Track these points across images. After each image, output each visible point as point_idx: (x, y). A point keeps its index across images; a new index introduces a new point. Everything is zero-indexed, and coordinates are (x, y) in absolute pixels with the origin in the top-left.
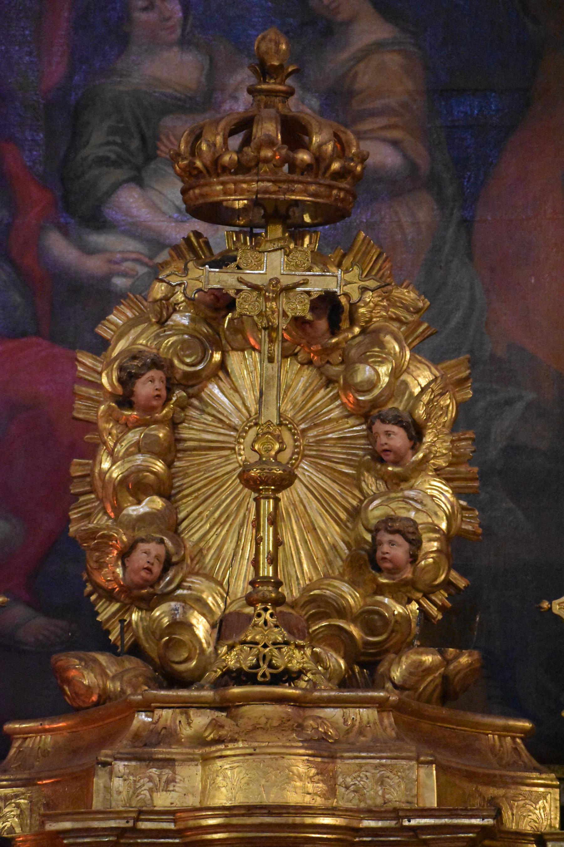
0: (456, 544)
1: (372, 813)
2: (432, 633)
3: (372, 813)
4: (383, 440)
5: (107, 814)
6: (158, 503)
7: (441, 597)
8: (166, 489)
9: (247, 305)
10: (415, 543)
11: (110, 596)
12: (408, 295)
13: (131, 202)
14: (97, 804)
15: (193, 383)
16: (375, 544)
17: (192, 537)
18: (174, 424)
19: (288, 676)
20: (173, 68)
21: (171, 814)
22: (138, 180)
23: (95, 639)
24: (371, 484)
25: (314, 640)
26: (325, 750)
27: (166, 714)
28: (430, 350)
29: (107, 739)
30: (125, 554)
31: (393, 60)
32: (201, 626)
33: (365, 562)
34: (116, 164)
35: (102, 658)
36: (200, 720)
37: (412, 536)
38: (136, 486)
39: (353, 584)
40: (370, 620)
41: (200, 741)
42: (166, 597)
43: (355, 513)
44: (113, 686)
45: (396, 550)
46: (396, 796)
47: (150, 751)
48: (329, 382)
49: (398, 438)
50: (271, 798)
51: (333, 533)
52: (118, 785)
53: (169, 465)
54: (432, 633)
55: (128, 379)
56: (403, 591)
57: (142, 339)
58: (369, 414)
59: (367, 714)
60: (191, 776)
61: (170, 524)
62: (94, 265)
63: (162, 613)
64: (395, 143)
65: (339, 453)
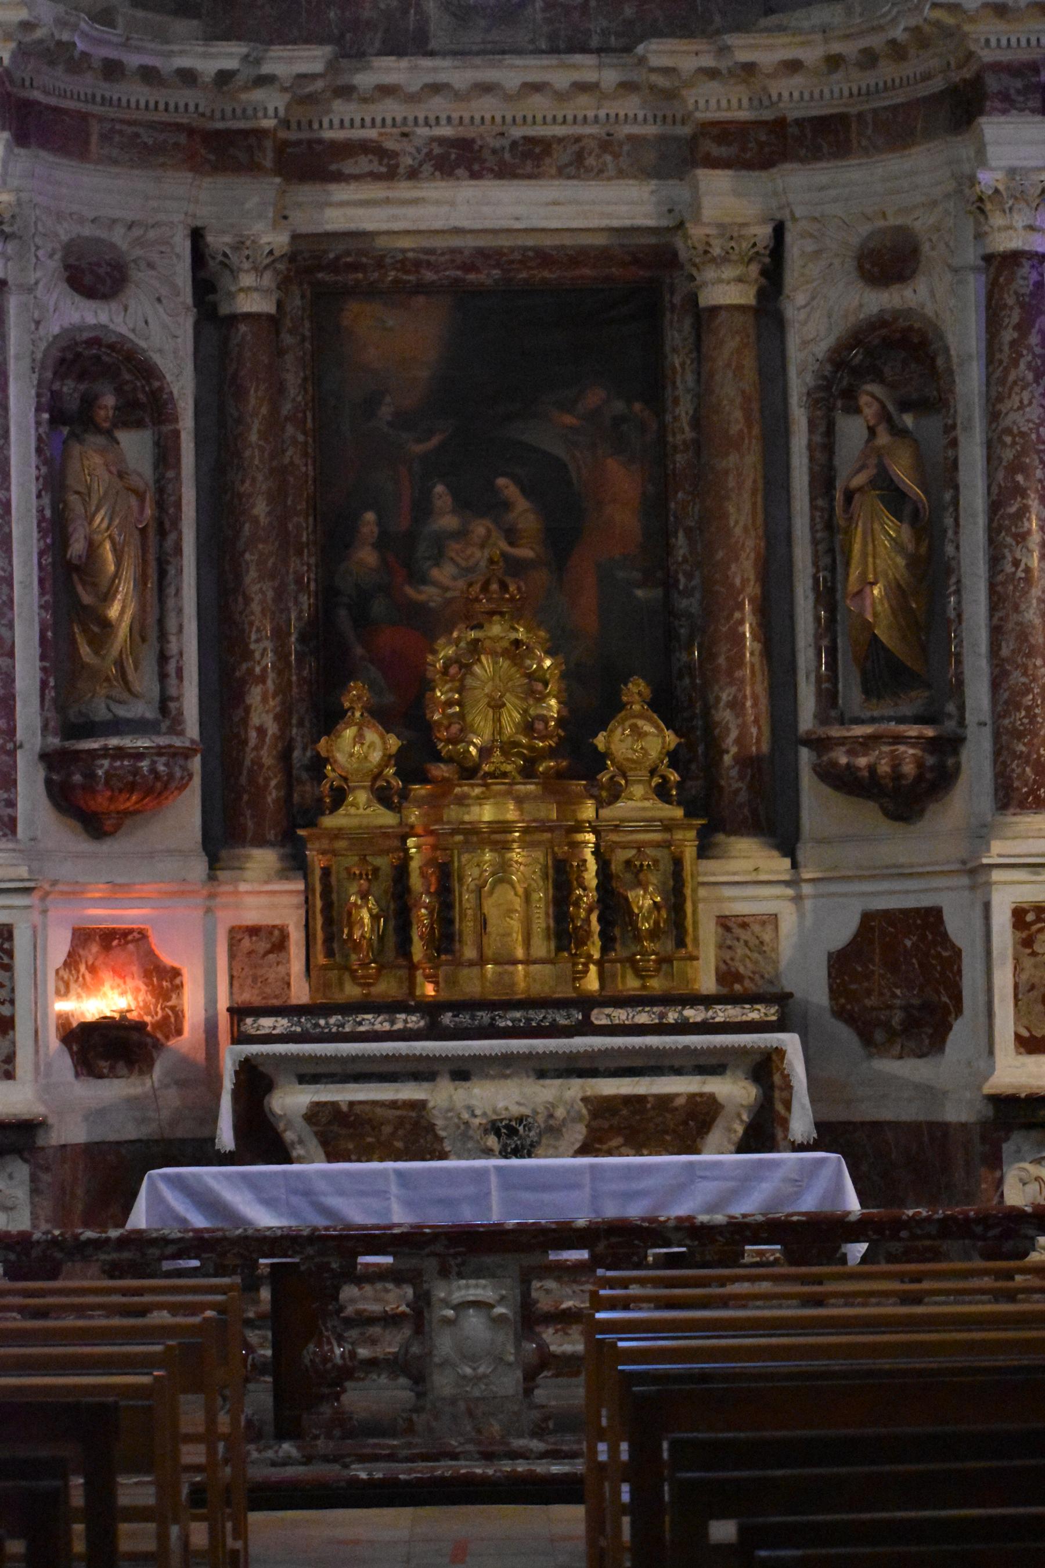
0: (561, 722)
1: (534, 821)
2: (552, 753)
3: (534, 821)
4: (534, 686)
5: (449, 822)
6: (457, 709)
7: (556, 739)
8: (459, 703)
9: (488, 643)
10: (546, 723)
11: (441, 741)
12: (542, 634)
13: (435, 573)
14: (445, 819)
15: (468, 667)
16: (533, 723)
17: (469, 718)
18: (462, 680)
19: (505, 775)
20: (448, 522)
21: (470, 823)
22: (437, 565)
23: (437, 757)
24: (531, 701)
25: (514, 755)
26: (520, 801)
27: (466, 789)
28: (549, 653)
29: (444, 795)
30: (447, 728)
31: (532, 517)
32: (473, 750)
33: (528, 727)
34: (429, 559)
35: (442, 765)
36: (477, 791)
37: (545, 720)
38: (450, 703)
39: (525, 736)
40: (532, 748)
41: (478, 798)
42: (462, 741)
43: (526, 711)
44: (446, 775)
45: (539, 726)
46: (542, 815)
47: (462, 801)
48: (515, 665)
49: (539, 686)
50: (501, 818)
51: (517, 717)
52: (452, 813)
53: (460, 694)
54: (552, 753)
55: (446, 667)
56: (542, 739)
57: (451, 651)
58: (530, 676)
59: (532, 787)
60: (475, 809)
61: (461, 716)
62: (422, 597)
63: (460, 747)
64: (532, 548)
65: (519, 690)
